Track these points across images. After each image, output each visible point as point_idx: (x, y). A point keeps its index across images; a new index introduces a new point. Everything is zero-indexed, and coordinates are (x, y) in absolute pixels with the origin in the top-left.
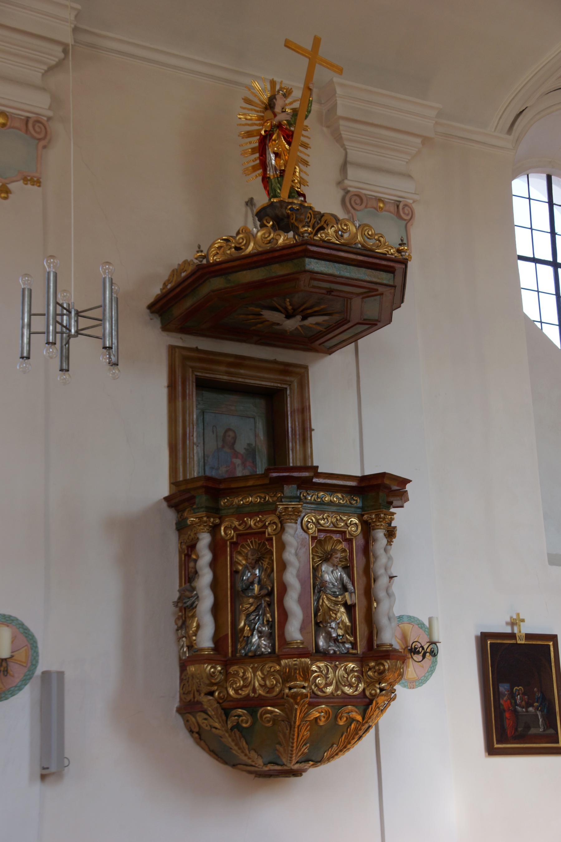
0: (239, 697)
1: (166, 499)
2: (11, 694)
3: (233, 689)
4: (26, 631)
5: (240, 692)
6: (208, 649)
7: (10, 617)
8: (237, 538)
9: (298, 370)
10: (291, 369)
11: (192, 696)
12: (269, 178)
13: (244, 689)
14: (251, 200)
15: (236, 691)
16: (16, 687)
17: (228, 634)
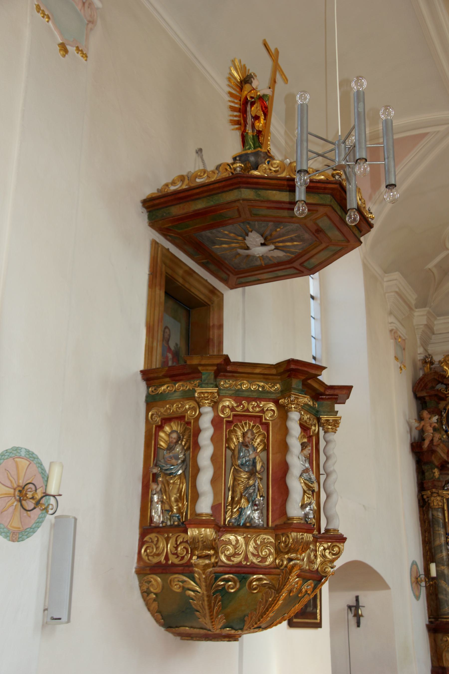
0: (230, 563)
1: (141, 371)
2: (26, 535)
3: (225, 555)
4: (43, 472)
5: (232, 559)
6: (207, 515)
7: (33, 453)
8: (233, 417)
9: (219, 294)
10: (216, 291)
11: (162, 559)
12: (248, 133)
13: (236, 556)
14: (201, 150)
15: (228, 558)
16: (31, 528)
17: (221, 504)
